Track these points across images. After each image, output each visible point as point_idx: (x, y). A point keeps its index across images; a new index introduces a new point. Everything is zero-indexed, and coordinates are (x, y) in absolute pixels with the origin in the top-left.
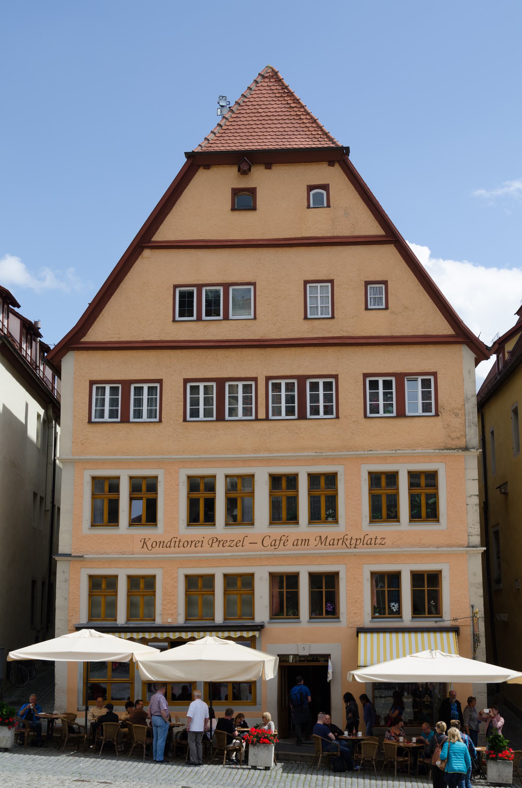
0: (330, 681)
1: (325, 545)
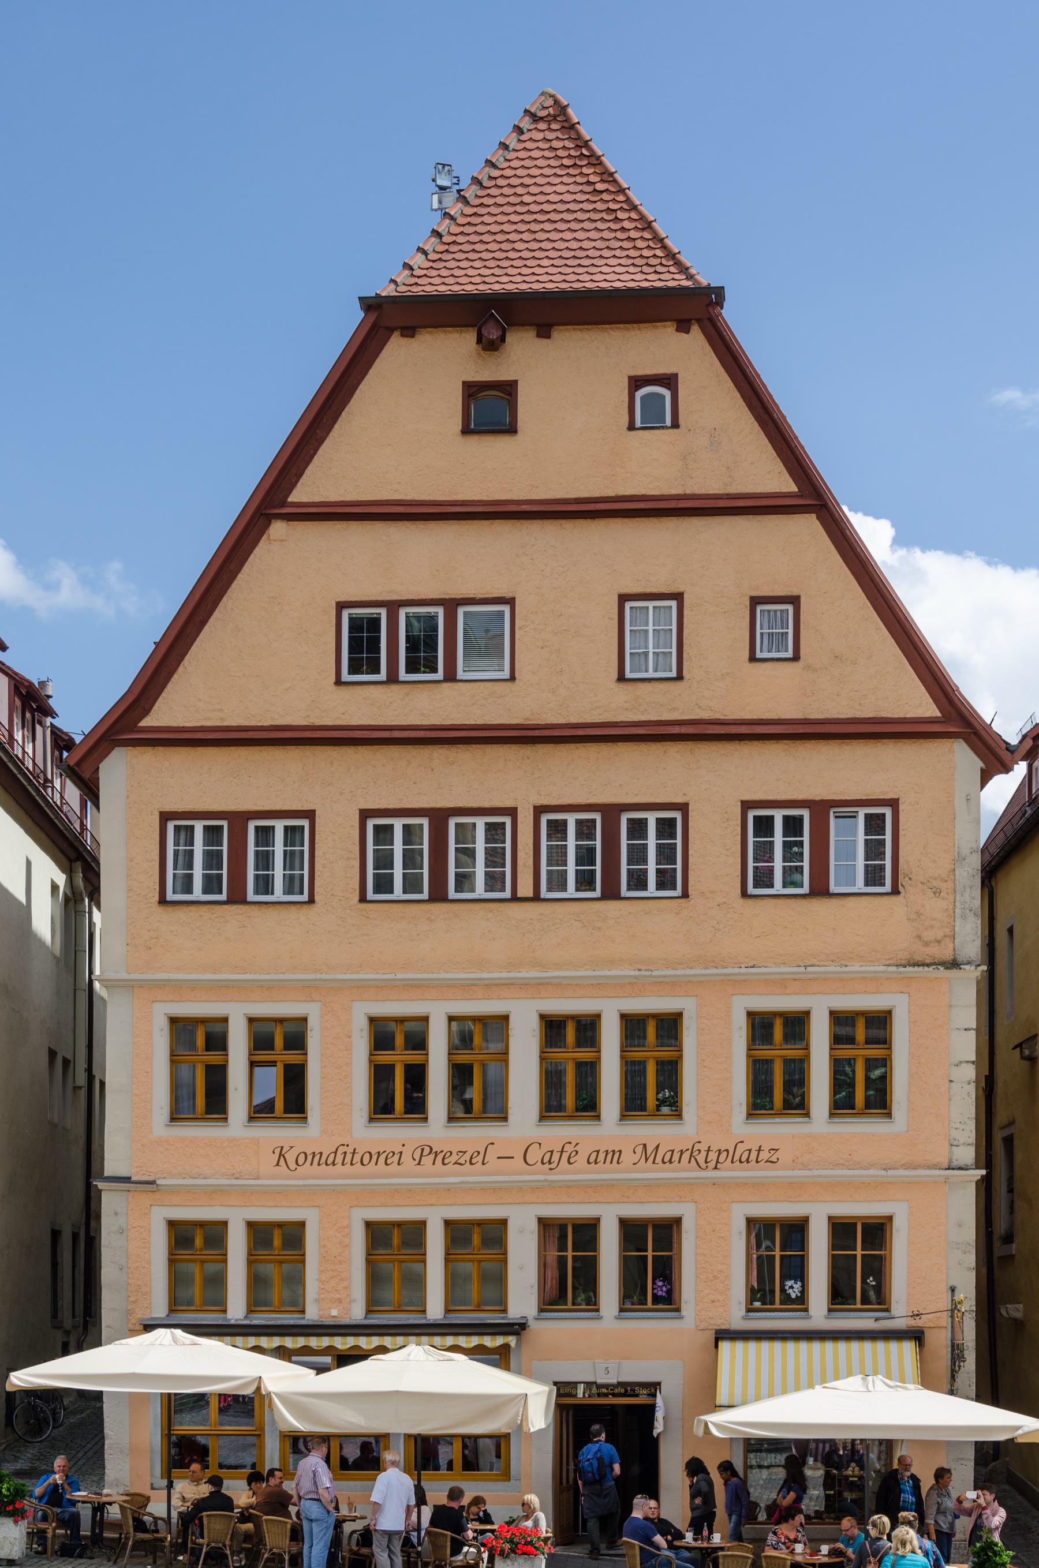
0: (659, 1435)
1: (654, 1163)
